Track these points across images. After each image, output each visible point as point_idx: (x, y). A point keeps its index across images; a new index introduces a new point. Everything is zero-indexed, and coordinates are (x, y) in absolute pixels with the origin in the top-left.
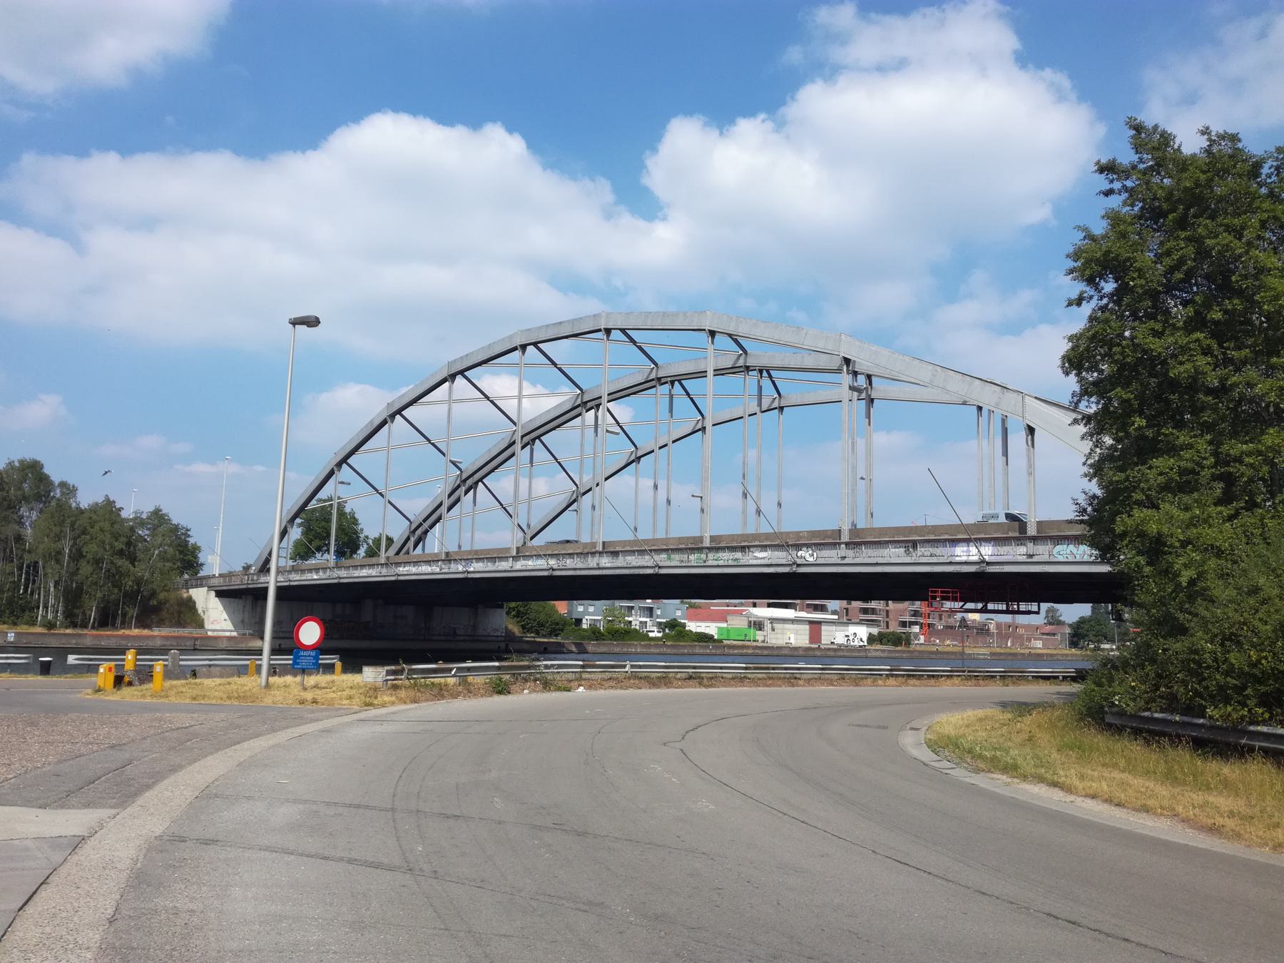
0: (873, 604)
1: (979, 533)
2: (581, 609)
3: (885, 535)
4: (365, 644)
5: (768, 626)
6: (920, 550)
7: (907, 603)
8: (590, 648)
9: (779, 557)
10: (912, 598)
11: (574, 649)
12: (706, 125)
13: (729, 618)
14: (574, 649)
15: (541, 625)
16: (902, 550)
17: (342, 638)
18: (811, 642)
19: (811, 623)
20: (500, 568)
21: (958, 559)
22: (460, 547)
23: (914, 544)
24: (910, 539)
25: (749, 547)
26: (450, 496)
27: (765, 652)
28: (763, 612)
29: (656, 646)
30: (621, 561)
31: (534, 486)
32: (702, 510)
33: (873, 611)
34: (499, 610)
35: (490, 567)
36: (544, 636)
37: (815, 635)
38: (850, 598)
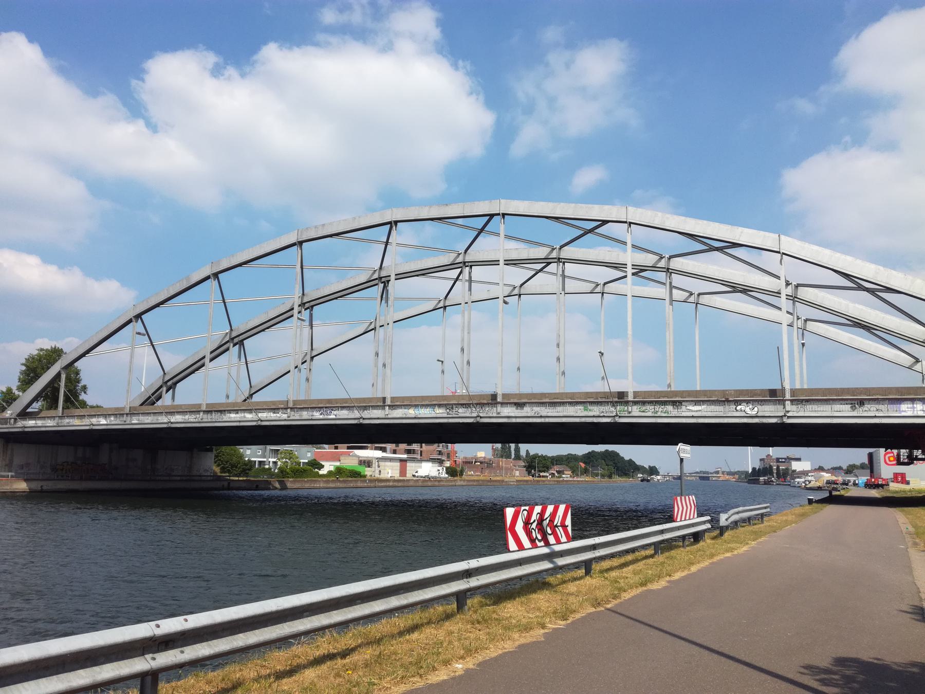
0: (415, 446)
1: (910, 394)
2: (248, 452)
3: (817, 395)
4: (116, 485)
5: (375, 464)
6: (867, 406)
7: (436, 445)
8: (289, 485)
9: (356, 414)
10: (439, 441)
11: (277, 485)
12: (281, 47)
13: (342, 458)
14: (277, 485)
15: (233, 466)
16: (582, 407)
17: (81, 479)
18: (401, 476)
19: (401, 460)
20: (373, 416)
21: (903, 414)
22: (228, 397)
23: (862, 403)
24: (858, 399)
25: (680, 402)
26: (211, 352)
27: (400, 484)
28: (370, 453)
29: (327, 482)
30: (527, 411)
31: (275, 349)
32: (443, 372)
33: (414, 452)
34: (209, 454)
35: (272, 415)
36: (236, 475)
37: (403, 472)
38: (397, 442)
